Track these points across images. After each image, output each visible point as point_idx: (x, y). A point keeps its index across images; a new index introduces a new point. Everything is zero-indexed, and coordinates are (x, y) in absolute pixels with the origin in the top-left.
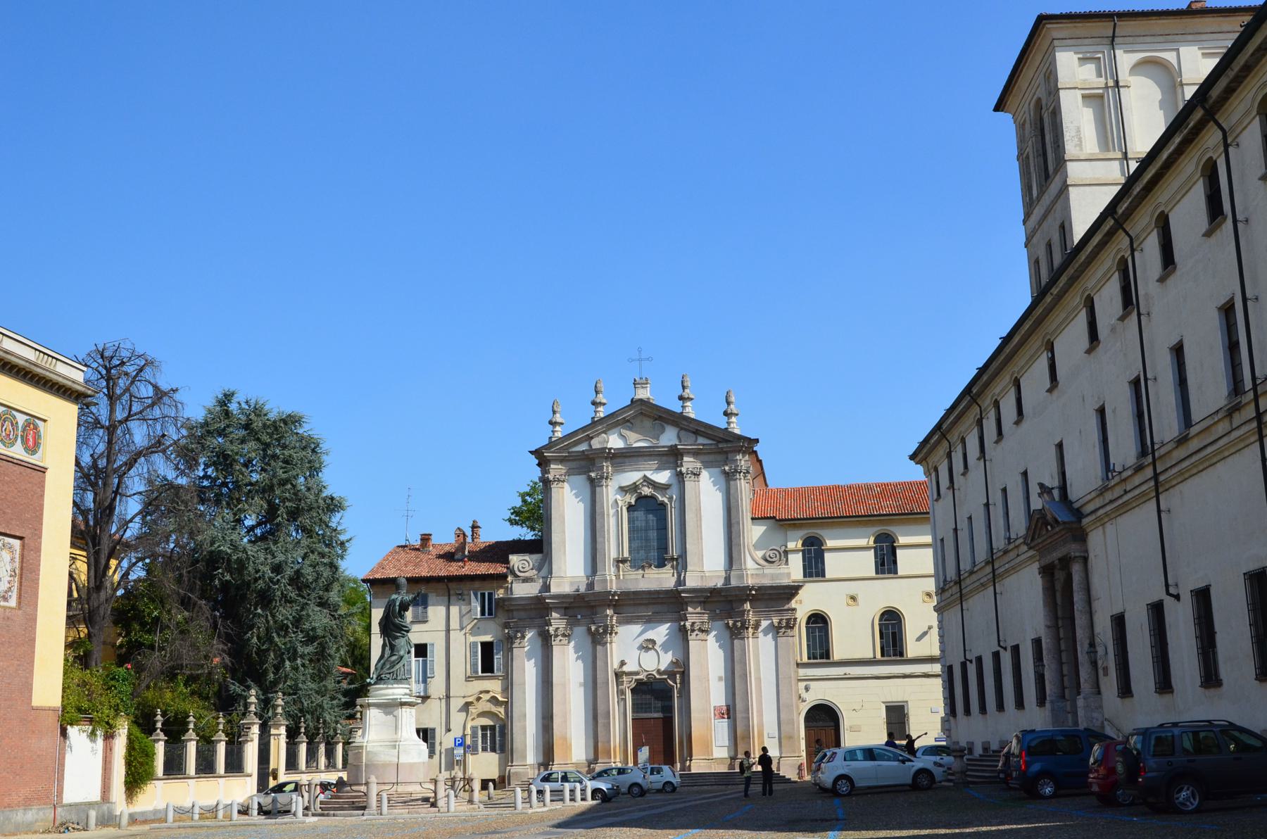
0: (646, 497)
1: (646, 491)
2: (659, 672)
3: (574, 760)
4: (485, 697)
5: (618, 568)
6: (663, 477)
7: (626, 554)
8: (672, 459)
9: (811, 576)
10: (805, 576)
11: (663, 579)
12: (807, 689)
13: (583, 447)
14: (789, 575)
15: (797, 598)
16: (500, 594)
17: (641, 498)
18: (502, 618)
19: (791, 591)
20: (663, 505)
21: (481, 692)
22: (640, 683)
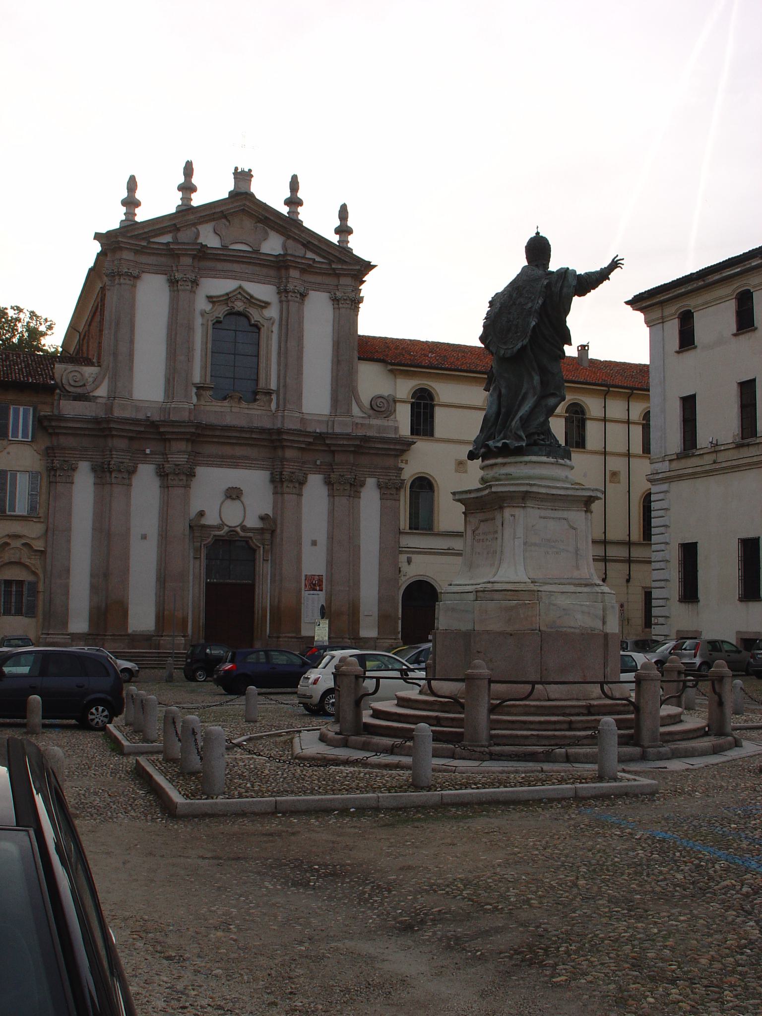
0: (239, 314)
1: (239, 306)
2: (244, 528)
3: (130, 631)
4: (17, 543)
5: (198, 396)
6: (262, 291)
7: (208, 380)
8: (272, 273)
9: (417, 434)
10: (412, 434)
11: (255, 415)
12: (409, 561)
13: (167, 239)
14: (396, 429)
15: (404, 457)
16: (45, 411)
17: (232, 313)
18: (44, 442)
19: (402, 447)
20: (257, 327)
21: (9, 536)
22: (218, 540)
